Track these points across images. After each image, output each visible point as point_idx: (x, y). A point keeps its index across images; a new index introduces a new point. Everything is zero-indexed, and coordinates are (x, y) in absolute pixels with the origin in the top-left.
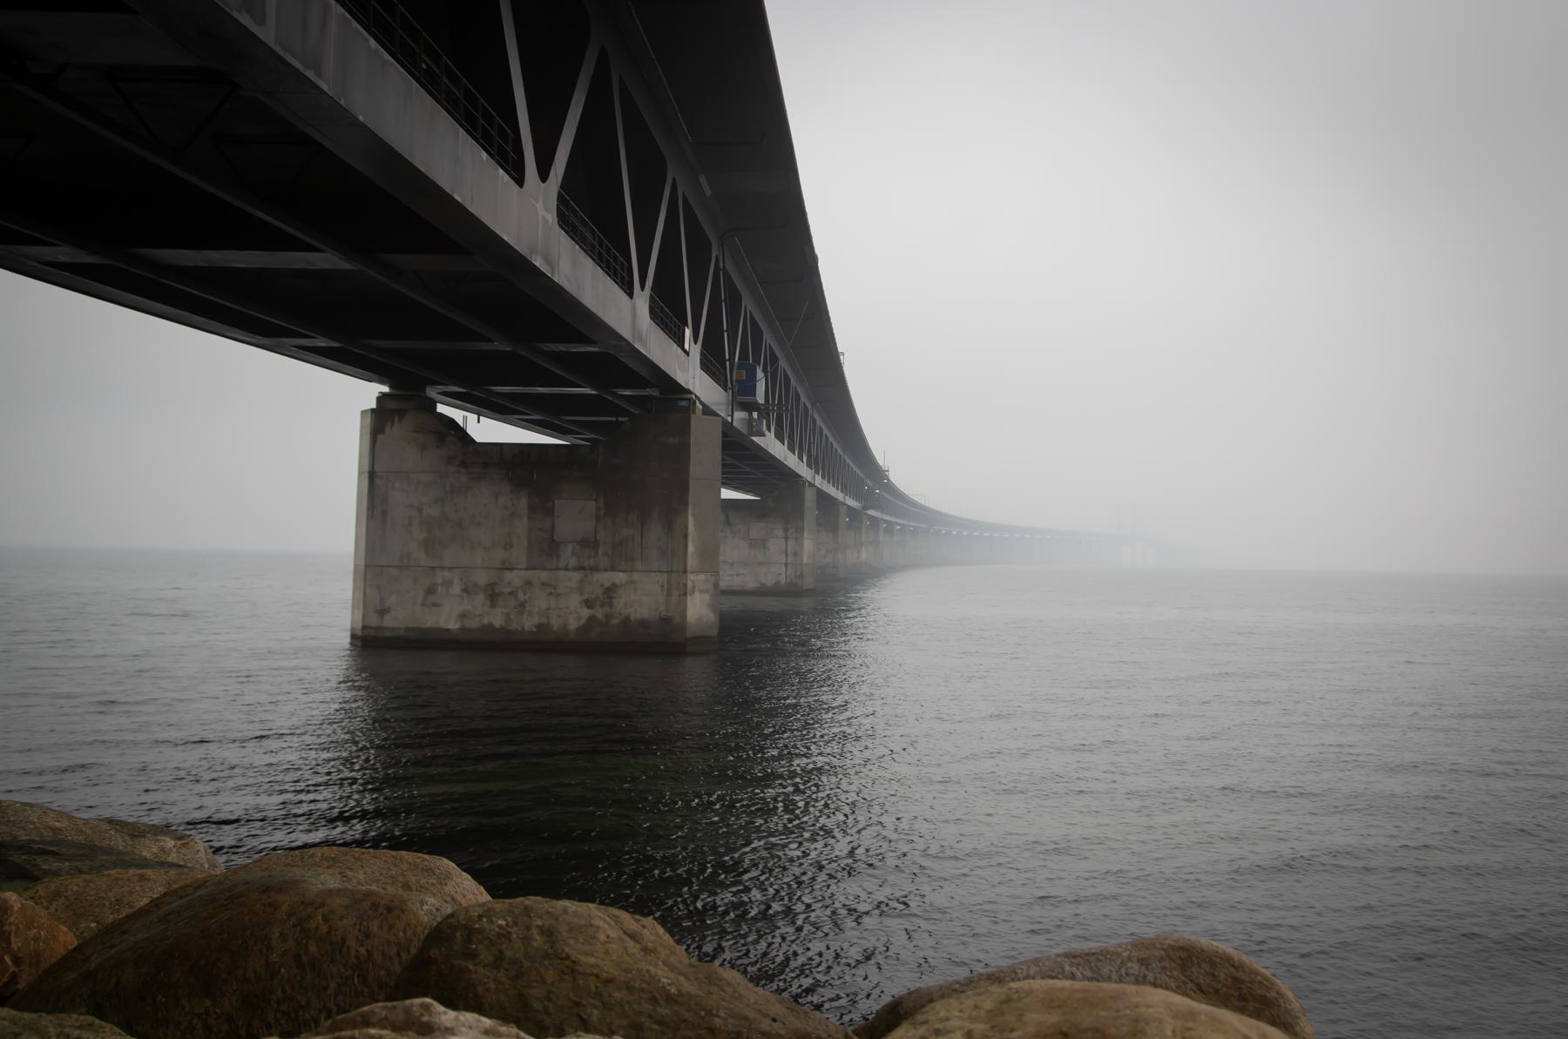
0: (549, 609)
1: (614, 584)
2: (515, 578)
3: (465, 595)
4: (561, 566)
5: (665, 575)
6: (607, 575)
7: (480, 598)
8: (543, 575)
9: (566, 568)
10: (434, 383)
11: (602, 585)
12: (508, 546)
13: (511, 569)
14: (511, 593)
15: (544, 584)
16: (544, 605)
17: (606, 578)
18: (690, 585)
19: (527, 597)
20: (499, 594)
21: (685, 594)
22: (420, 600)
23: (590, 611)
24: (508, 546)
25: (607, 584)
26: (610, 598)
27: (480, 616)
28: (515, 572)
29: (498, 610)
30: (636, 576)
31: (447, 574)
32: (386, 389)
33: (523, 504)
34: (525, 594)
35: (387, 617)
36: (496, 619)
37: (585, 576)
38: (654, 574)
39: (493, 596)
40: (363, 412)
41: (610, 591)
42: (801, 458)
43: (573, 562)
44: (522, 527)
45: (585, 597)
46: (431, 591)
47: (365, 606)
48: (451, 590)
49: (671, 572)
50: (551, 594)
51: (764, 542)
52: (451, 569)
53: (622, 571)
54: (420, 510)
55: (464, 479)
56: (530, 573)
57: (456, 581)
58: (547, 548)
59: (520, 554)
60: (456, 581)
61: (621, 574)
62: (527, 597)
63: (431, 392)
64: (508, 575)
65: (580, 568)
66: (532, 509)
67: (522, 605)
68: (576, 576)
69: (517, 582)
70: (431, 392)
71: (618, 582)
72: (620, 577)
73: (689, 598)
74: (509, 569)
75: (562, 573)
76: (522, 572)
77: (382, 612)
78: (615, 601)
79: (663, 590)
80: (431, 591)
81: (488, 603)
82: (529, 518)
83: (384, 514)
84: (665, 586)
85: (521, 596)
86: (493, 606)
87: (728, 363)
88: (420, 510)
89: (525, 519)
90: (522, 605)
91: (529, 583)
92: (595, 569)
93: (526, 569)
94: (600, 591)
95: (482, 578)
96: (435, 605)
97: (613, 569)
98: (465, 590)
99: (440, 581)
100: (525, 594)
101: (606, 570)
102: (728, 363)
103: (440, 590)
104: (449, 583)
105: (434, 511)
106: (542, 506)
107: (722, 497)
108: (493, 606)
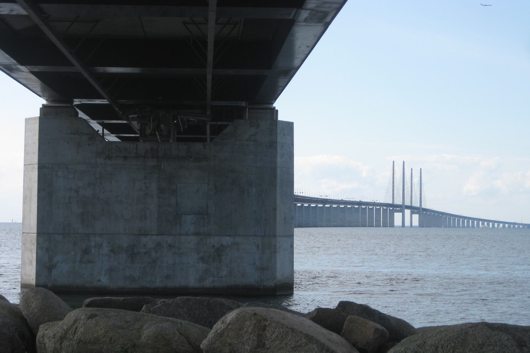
1: (222, 245)
2: (149, 241)
8: (169, 239)
9: (187, 235)
13: (146, 235)
14: (145, 253)
15: (170, 246)
17: (214, 241)
18: (278, 245)
21: (275, 252)
28: (149, 237)
31: (98, 239)
37: (201, 240)
40: (27, 120)
41: (219, 251)
46: (86, 252)
53: (228, 236)
54: (77, 191)
61: (228, 238)
65: (197, 234)
68: (194, 239)
72: (227, 240)
73: (277, 255)
74: (144, 235)
76: (154, 237)
85: (153, 254)
88: (77, 191)
91: (159, 245)
93: (157, 235)
96: (89, 262)
98: (112, 251)
99: (93, 244)
100: (156, 253)
107: (402, 213)
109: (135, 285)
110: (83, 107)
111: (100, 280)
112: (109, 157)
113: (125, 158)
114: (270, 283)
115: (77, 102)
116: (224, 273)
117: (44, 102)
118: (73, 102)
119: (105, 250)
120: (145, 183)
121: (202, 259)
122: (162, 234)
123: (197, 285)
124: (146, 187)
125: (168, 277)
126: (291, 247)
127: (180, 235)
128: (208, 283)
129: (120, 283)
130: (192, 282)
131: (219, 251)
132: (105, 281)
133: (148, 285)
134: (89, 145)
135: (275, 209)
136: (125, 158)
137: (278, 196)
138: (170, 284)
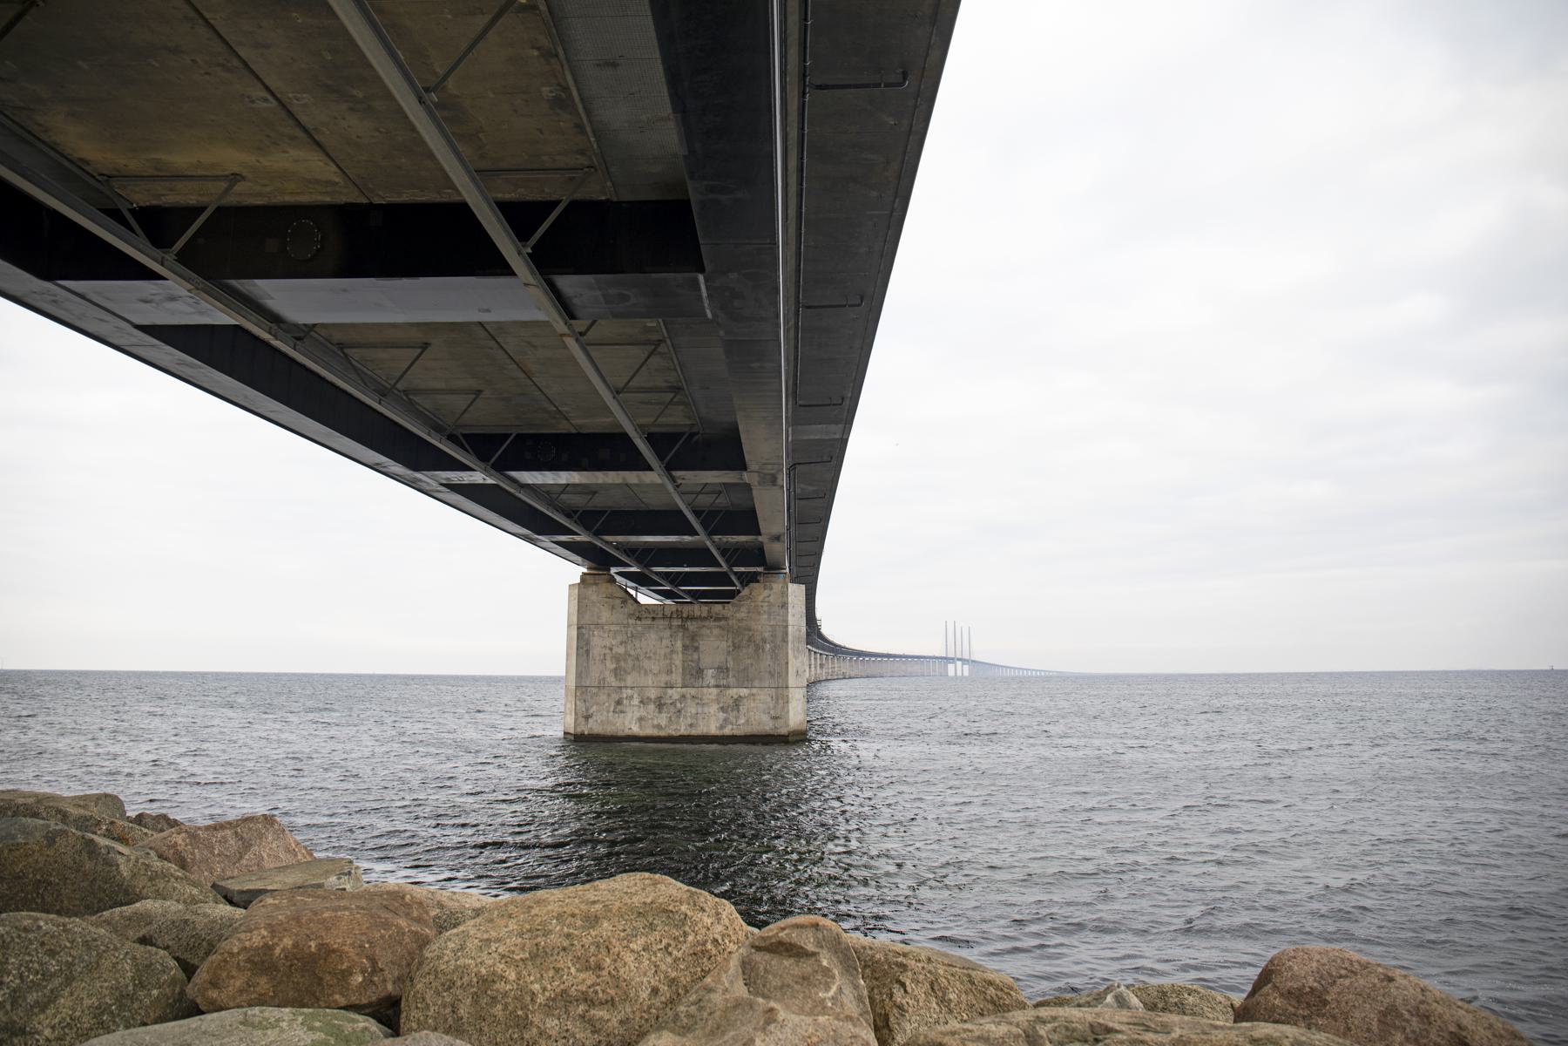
1: (740, 697)
2: (674, 694)
4: (704, 685)
5: (773, 690)
7: (652, 707)
8: (693, 691)
9: (708, 687)
12: (669, 672)
13: (672, 687)
16: (694, 711)
17: (733, 692)
20: (665, 704)
22: (612, 709)
24: (669, 672)
25: (735, 697)
27: (652, 719)
29: (664, 715)
30: (754, 691)
31: (629, 691)
32: (585, 570)
33: (679, 644)
35: (590, 720)
36: (662, 720)
39: (660, 706)
41: (737, 702)
43: (713, 682)
44: (678, 660)
46: (619, 703)
47: (576, 714)
52: (632, 688)
54: (611, 649)
55: (639, 629)
56: (684, 690)
58: (694, 673)
59: (677, 678)
64: (670, 691)
65: (717, 686)
66: (685, 647)
67: (679, 711)
68: (714, 691)
69: (676, 697)
72: (743, 692)
75: (705, 690)
77: (587, 718)
82: (683, 653)
83: (588, 652)
85: (678, 705)
86: (660, 712)
88: (611, 649)
89: (680, 655)
90: (679, 711)
91: (683, 696)
95: (653, 694)
96: (622, 712)
98: (641, 702)
99: (625, 696)
103: (625, 702)
104: (632, 697)
105: (621, 650)
106: (692, 645)
108: (660, 712)
109: (662, 733)
110: (619, 574)
112: (639, 618)
113: (654, 619)
114: (784, 731)
115: (613, 570)
116: (742, 721)
117: (585, 570)
118: (609, 570)
119: (636, 701)
121: (722, 709)
123: (718, 733)
125: (691, 725)
128: (727, 731)
129: (649, 731)
130: (713, 729)
131: (737, 702)
132: (636, 729)
133: (674, 733)
135: (787, 663)
136: (654, 619)
137: (790, 652)
138: (694, 732)
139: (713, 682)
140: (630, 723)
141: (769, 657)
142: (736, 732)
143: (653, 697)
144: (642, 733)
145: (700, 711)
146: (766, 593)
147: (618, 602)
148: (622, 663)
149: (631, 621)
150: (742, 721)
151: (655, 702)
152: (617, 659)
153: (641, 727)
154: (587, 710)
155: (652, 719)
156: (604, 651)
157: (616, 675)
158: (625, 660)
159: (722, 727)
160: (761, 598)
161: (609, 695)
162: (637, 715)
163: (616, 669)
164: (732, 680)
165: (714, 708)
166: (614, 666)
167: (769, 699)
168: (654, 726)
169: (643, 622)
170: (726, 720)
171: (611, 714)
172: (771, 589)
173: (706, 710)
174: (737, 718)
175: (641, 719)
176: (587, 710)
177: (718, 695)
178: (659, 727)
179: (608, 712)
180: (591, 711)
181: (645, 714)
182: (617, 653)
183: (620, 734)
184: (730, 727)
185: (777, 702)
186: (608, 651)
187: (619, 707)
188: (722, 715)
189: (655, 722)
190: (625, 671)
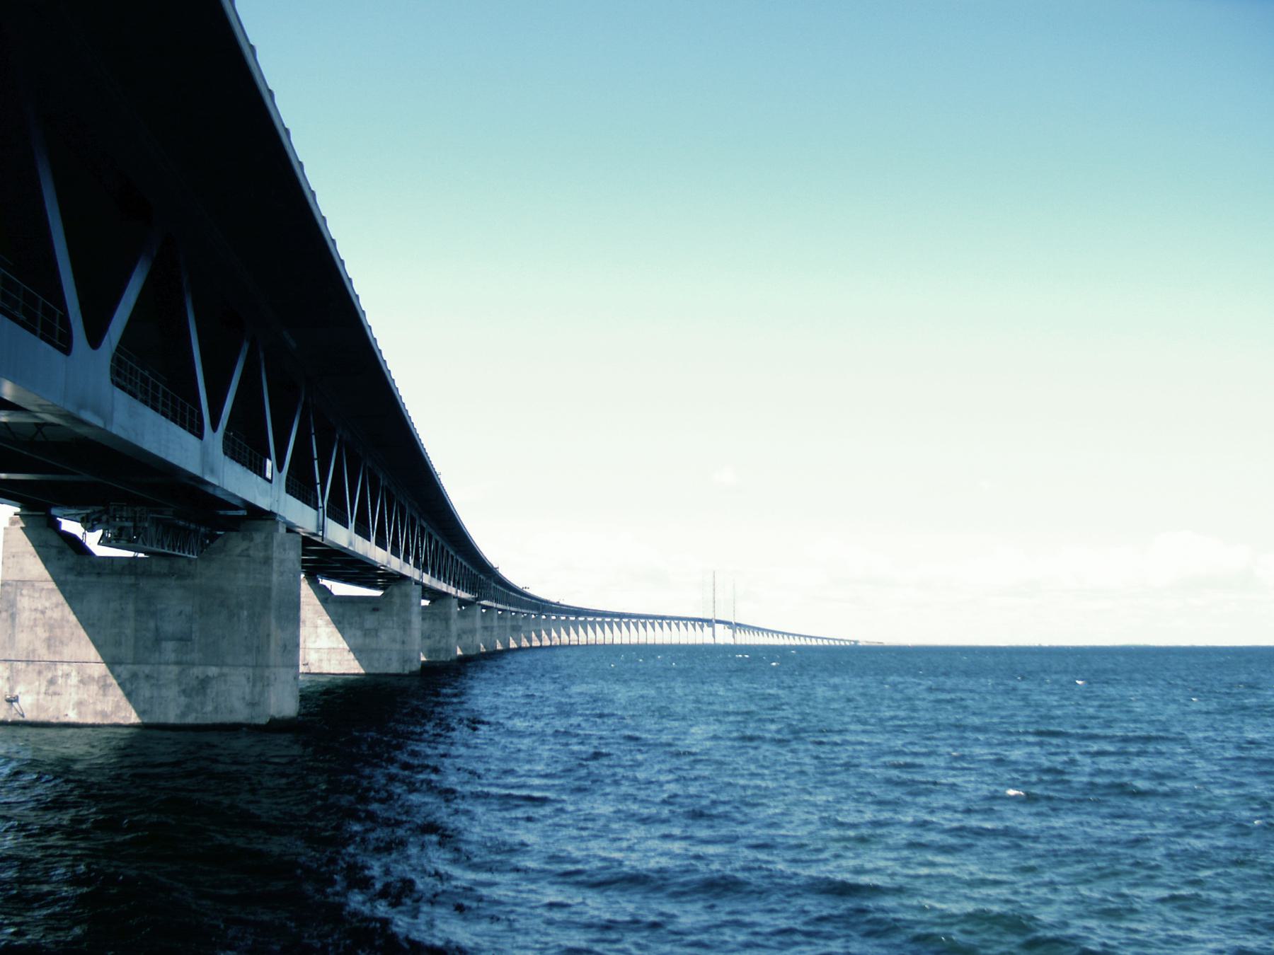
0: (152, 698)
1: (207, 676)
3: (81, 685)
5: (251, 670)
6: (201, 668)
7: (94, 688)
8: (147, 669)
9: (167, 663)
10: (56, 506)
11: (197, 677)
12: (118, 644)
16: (148, 694)
17: (197, 671)
19: (134, 687)
22: (43, 690)
23: (187, 700)
24: (118, 644)
25: (201, 677)
26: (204, 688)
28: (123, 666)
30: (225, 670)
31: (65, 667)
33: (130, 608)
34: (132, 685)
38: (241, 669)
41: (204, 683)
42: (406, 560)
45: (183, 687)
46: (52, 682)
48: (69, 681)
49: (256, 666)
50: (153, 685)
51: (376, 631)
54: (43, 612)
56: (135, 668)
57: (74, 674)
60: (74, 674)
62: (134, 687)
63: (54, 511)
65: (178, 663)
66: (139, 612)
68: (175, 669)
70: (54, 511)
71: (210, 674)
72: (213, 671)
75: (162, 668)
76: (129, 667)
78: (209, 691)
79: (248, 682)
80: (52, 682)
81: (101, 692)
84: (251, 679)
86: (105, 695)
87: (318, 486)
88: (43, 612)
92: (193, 664)
94: (195, 683)
96: (55, 694)
97: (207, 664)
98: (82, 681)
99: (60, 673)
100: (132, 685)
101: (200, 665)
102: (318, 486)
103: (60, 681)
104: (67, 675)
108: (105, 695)
111: (67, 715)
112: (80, 574)
116: (209, 708)
119: (74, 680)
120: (121, 604)
121: (184, 691)
122: (139, 663)
123: (177, 721)
124: (122, 609)
126: (295, 678)
127: (160, 663)
128: (191, 719)
131: (204, 683)
132: (73, 717)
134: (59, 559)
135: (268, 636)
139: (172, 657)
140: (66, 708)
141: (245, 627)
142: (199, 721)
143: (96, 675)
144: (81, 721)
145: (155, 694)
146: (244, 545)
147: (54, 552)
148: (58, 632)
149: (71, 577)
150: (209, 708)
151: (98, 682)
152: (51, 627)
153: (80, 713)
154: (12, 689)
155: (94, 703)
156: (34, 615)
157: (49, 647)
158: (62, 627)
159: (184, 714)
160: (238, 550)
161: (40, 673)
162: (75, 698)
163: (49, 639)
164: (196, 656)
165: (172, 692)
166: (46, 635)
167: (244, 681)
168: (96, 713)
169: (86, 579)
170: (188, 706)
171: (42, 696)
172: (252, 540)
173: (164, 692)
174: (203, 704)
175: (80, 704)
176: (12, 689)
177: (181, 673)
178: (103, 713)
179: (38, 693)
180: (16, 693)
181: (85, 696)
182: (51, 618)
183: (54, 721)
184: (194, 715)
185: (254, 686)
186: (39, 615)
187: (52, 689)
188: (183, 700)
189: (99, 708)
190: (62, 642)
